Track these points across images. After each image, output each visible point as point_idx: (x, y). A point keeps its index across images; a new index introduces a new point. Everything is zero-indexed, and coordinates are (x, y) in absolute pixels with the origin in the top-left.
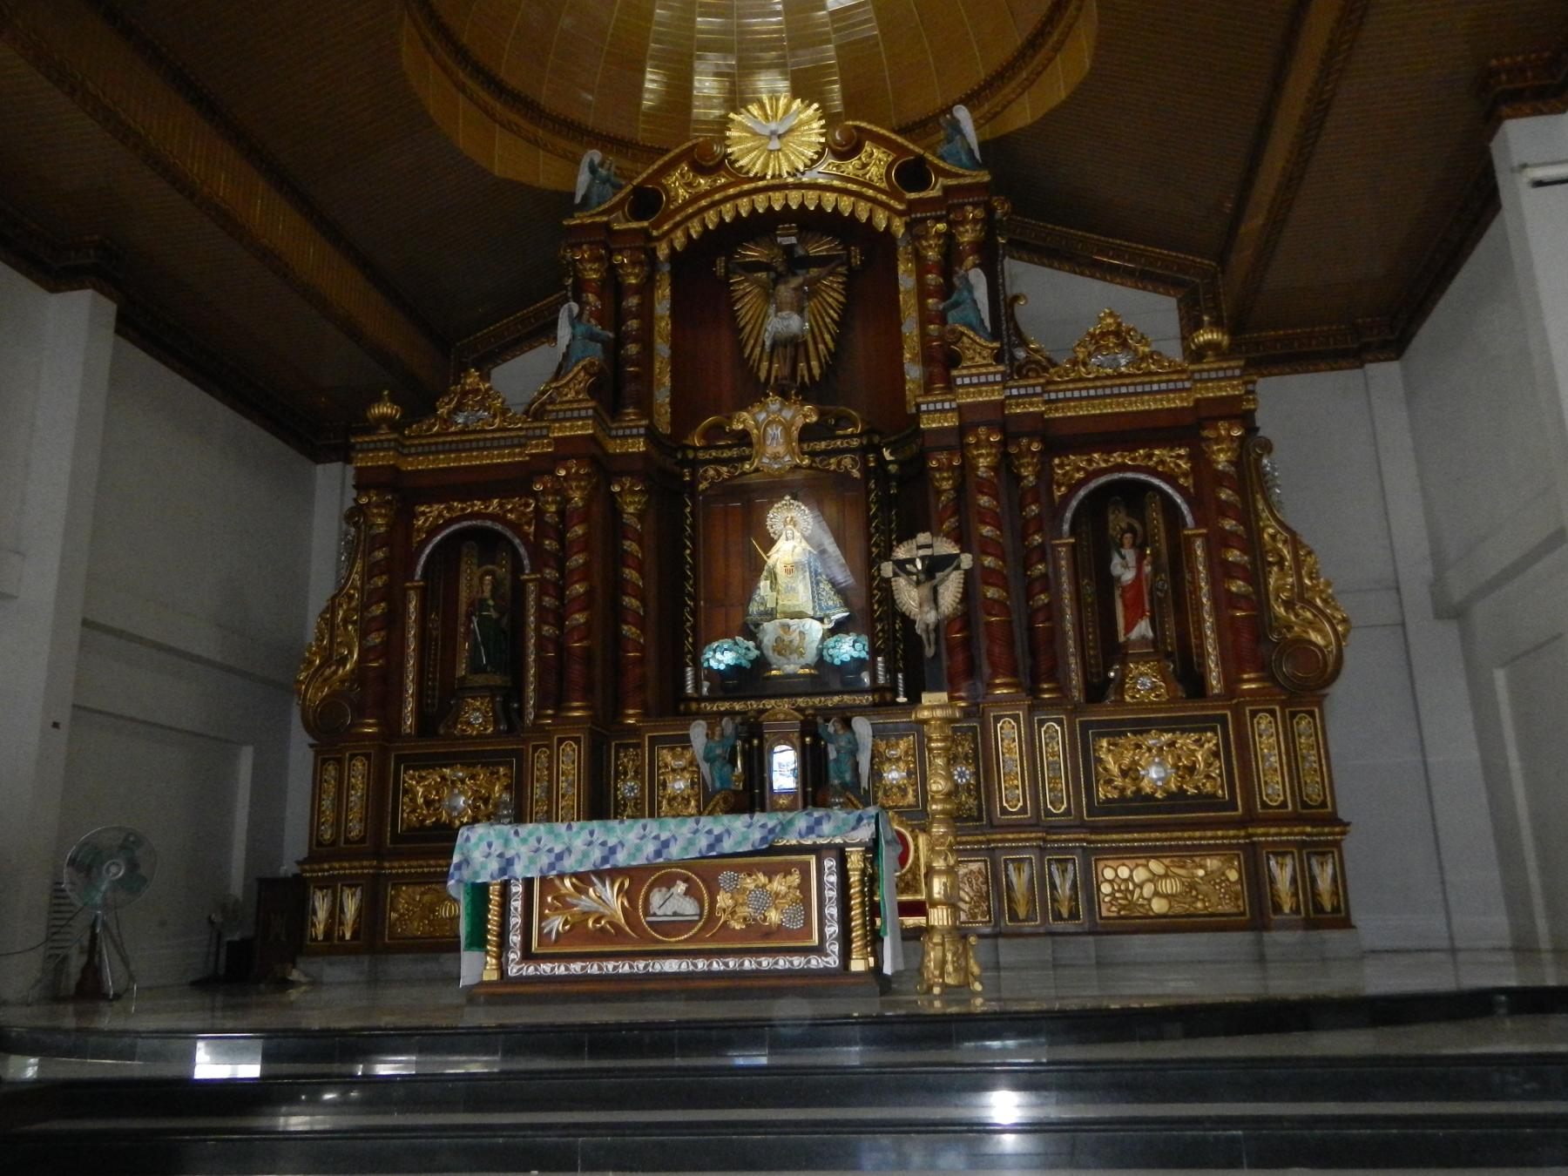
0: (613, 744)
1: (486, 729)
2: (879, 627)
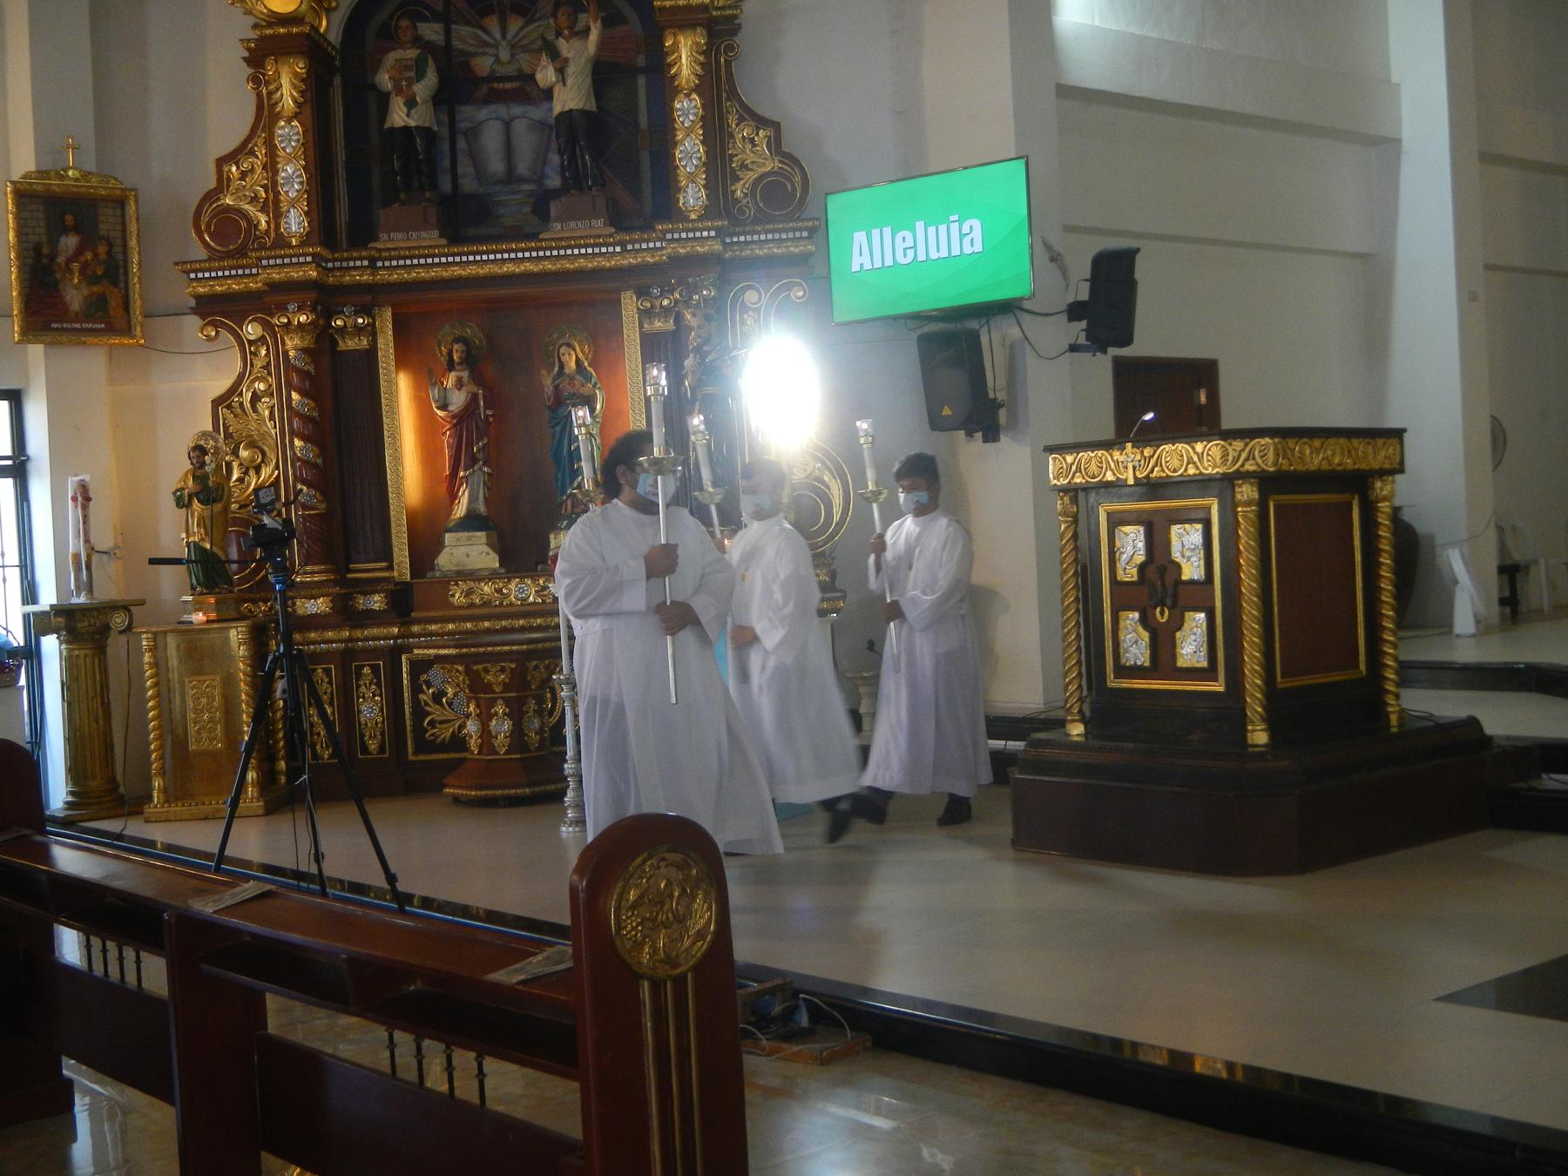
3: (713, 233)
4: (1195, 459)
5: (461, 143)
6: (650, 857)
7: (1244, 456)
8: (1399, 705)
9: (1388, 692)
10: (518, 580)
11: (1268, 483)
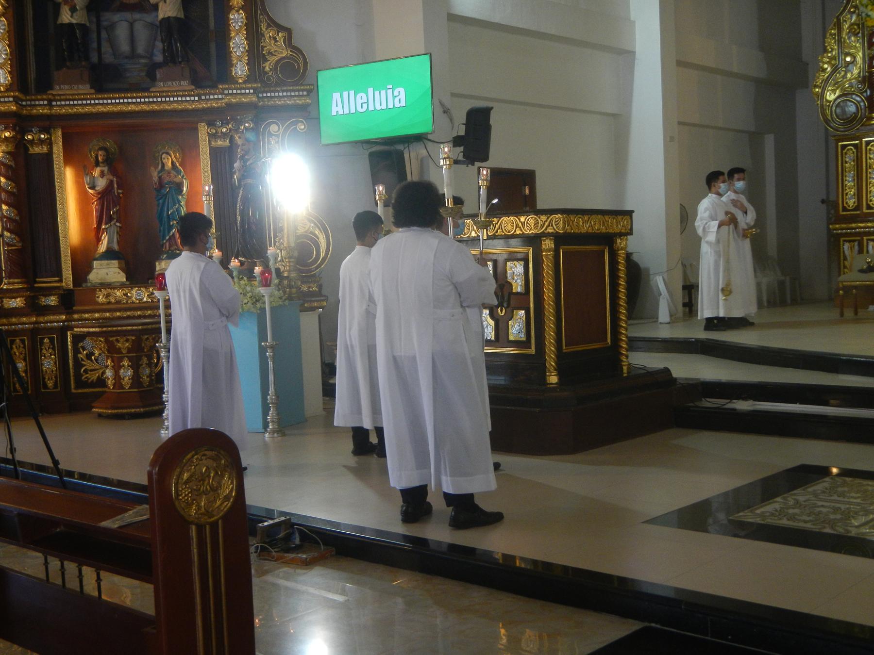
3: (252, 91)
4: (520, 225)
5: (104, 35)
6: (196, 454)
7: (547, 224)
8: (628, 362)
9: (623, 354)
10: (136, 288)
11: (560, 239)
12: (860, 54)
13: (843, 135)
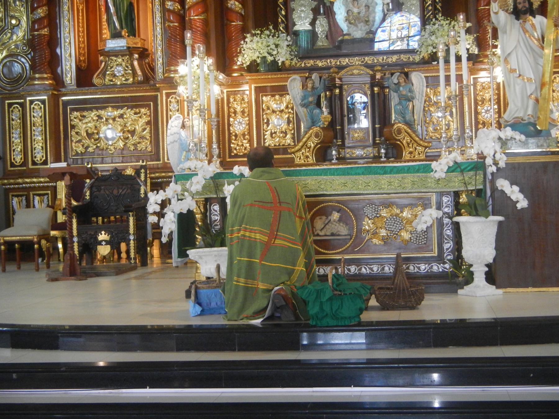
0: (225, 91)
1: (127, 80)
2: (430, 2)
12: (25, 18)
13: (9, 94)
